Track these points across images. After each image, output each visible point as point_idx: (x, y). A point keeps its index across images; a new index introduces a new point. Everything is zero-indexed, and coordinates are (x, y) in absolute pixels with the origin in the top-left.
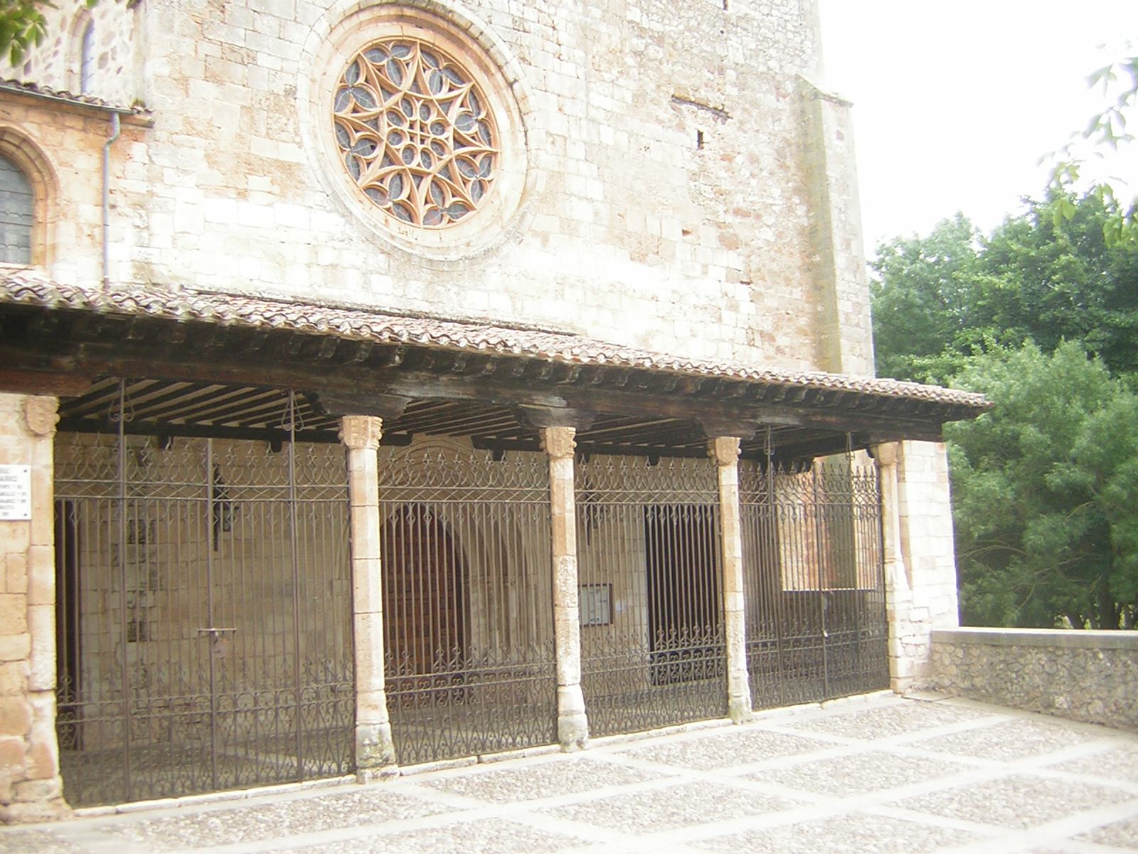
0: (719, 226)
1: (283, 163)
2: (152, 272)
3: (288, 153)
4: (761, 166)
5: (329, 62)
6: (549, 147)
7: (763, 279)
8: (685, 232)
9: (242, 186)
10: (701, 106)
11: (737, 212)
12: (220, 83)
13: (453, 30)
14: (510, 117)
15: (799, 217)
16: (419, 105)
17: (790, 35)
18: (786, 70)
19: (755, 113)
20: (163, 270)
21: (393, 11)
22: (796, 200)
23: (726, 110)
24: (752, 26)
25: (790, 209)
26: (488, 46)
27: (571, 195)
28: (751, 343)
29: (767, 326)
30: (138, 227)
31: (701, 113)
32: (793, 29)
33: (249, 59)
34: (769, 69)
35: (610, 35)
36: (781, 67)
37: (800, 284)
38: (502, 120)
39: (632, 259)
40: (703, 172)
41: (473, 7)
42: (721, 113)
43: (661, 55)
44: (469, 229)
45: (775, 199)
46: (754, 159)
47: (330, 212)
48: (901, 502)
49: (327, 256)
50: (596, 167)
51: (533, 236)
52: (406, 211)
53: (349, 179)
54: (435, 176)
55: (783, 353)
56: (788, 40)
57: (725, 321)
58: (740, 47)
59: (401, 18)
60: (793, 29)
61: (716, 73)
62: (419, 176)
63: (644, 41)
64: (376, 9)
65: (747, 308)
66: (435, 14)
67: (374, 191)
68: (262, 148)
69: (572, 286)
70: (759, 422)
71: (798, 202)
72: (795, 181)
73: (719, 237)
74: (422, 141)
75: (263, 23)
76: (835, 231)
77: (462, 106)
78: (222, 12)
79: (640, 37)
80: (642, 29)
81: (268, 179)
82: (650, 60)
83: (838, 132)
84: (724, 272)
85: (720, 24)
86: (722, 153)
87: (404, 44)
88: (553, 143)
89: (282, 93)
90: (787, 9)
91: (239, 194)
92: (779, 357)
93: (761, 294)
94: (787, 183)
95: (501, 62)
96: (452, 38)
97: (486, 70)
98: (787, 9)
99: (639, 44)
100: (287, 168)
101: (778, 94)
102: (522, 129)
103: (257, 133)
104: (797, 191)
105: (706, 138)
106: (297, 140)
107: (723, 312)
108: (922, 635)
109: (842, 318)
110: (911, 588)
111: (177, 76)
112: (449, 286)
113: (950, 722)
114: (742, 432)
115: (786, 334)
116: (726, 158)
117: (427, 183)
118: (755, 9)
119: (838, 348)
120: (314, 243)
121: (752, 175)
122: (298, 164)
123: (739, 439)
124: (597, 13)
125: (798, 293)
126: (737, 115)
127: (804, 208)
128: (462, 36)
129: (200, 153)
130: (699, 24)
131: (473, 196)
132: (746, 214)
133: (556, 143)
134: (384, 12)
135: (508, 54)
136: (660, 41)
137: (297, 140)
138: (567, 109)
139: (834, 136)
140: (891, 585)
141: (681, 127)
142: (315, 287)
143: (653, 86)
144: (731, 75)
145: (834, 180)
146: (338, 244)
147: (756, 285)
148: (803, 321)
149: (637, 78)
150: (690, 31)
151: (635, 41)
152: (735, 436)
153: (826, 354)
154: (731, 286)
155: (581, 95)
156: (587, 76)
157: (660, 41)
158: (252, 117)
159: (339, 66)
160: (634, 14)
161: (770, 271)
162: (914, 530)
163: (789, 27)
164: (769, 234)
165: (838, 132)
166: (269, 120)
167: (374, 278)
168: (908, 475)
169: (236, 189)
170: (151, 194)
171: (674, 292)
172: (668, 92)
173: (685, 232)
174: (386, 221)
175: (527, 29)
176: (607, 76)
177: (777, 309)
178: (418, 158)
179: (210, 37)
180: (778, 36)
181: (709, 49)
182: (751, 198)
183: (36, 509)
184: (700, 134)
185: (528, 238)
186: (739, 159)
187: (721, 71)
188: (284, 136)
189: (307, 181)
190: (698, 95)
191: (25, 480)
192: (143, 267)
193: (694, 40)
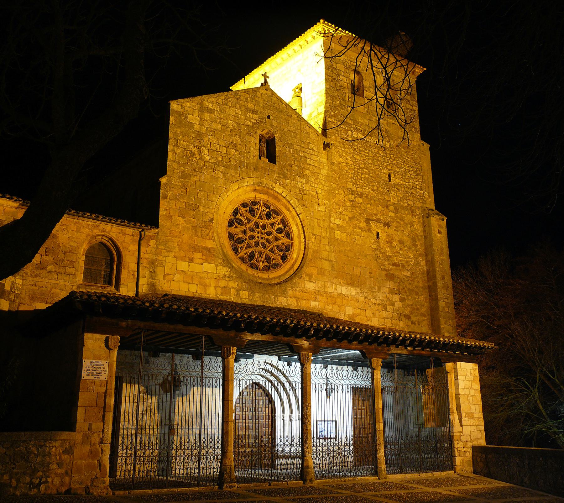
0: (386, 270)
1: (207, 248)
2: (155, 289)
3: (209, 244)
4: (405, 245)
5: (226, 209)
7: (406, 292)
9: (191, 257)
10: (378, 221)
12: (184, 218)
13: (276, 194)
14: (298, 228)
17: (418, 190)
19: (402, 223)
20: (160, 288)
22: (420, 259)
24: (401, 187)
25: (417, 263)
26: (289, 200)
27: (322, 259)
28: (399, 318)
29: (407, 312)
30: (151, 272)
31: (378, 224)
32: (420, 188)
34: (409, 205)
35: (340, 195)
36: (414, 203)
38: (294, 229)
39: (348, 284)
40: (379, 249)
41: (283, 185)
42: (387, 225)
43: (361, 201)
45: (411, 259)
46: (401, 242)
47: (224, 267)
48: (457, 388)
49: (223, 283)
51: (306, 275)
52: (255, 267)
53: (233, 253)
55: (415, 324)
56: (417, 192)
57: (388, 310)
58: (396, 196)
60: (420, 188)
63: (354, 196)
64: (245, 187)
65: (398, 304)
66: (268, 188)
70: (390, 352)
73: (386, 275)
75: (201, 194)
76: (437, 272)
77: (279, 224)
79: (353, 194)
80: (353, 191)
81: (201, 254)
83: (439, 230)
84: (388, 289)
86: (387, 240)
89: (207, 221)
91: (190, 259)
92: (413, 325)
93: (405, 299)
94: (417, 252)
96: (276, 198)
97: (289, 210)
100: (208, 250)
101: (413, 215)
102: (303, 233)
103: (197, 236)
104: (420, 255)
106: (213, 238)
107: (387, 306)
108: (467, 448)
109: (441, 309)
110: (462, 426)
112: (271, 295)
113: (473, 484)
114: (382, 357)
115: (416, 316)
116: (390, 242)
118: (403, 181)
119: (439, 321)
120: (218, 278)
121: (401, 249)
122: (213, 248)
123: (381, 359)
124: (335, 186)
125: (421, 298)
126: (395, 224)
127: (424, 262)
128: (279, 196)
129: (176, 245)
130: (378, 188)
131: (282, 259)
134: (248, 188)
136: (361, 195)
137: (213, 238)
138: (321, 224)
139: (437, 233)
140: (452, 424)
141: (369, 230)
142: (218, 296)
143: (357, 214)
144: (391, 208)
146: (227, 279)
147: (402, 295)
148: (423, 310)
149: (351, 211)
150: (374, 191)
151: (350, 196)
152: (380, 358)
153: (435, 326)
154: (391, 296)
155: (327, 219)
156: (330, 211)
157: (361, 195)
158: (196, 230)
159: (230, 210)
160: (350, 185)
161: (409, 289)
162: (462, 400)
163: (418, 187)
164: (408, 274)
165: (439, 230)
167: (241, 292)
168: (459, 377)
169: (189, 257)
170: (157, 260)
171: (366, 298)
172: (364, 217)
174: (247, 269)
177: (412, 305)
179: (181, 200)
180: (413, 191)
181: (382, 198)
182: (400, 258)
183: (110, 377)
184: (378, 234)
185: (304, 276)
186: (395, 243)
187: (387, 207)
189: (216, 254)
190: (377, 217)
191: (106, 366)
192: (152, 286)
193: (376, 195)
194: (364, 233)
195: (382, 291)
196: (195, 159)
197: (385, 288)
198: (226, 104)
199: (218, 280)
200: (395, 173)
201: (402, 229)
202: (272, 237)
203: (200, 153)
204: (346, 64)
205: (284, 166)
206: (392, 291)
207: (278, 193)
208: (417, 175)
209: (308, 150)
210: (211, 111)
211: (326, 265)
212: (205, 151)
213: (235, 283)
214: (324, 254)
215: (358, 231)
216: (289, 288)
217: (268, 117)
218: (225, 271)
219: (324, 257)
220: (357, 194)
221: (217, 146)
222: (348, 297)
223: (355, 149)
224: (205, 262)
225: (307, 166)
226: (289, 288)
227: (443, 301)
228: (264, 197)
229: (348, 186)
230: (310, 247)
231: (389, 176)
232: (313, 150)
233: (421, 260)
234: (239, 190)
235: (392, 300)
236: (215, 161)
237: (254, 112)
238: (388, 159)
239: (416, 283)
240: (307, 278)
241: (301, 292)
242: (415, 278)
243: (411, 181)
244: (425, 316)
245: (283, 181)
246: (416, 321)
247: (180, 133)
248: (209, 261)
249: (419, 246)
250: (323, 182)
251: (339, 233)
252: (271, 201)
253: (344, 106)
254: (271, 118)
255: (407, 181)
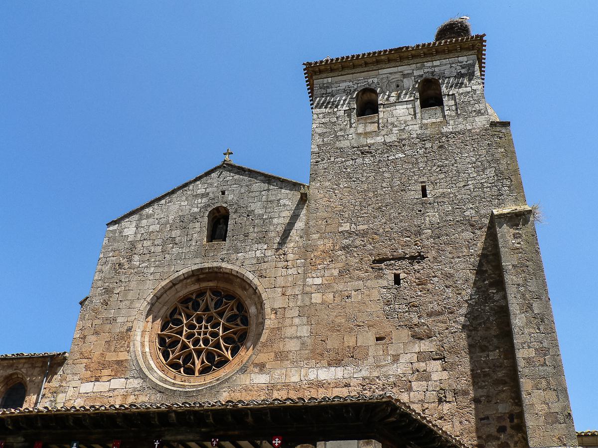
3: (123, 356)
6: (273, 316)
8: (378, 339)
11: (430, 315)
13: (226, 276)
15: (497, 301)
16: (205, 317)
18: (482, 212)
19: (449, 249)
21: (193, 279)
23: (422, 254)
27: (284, 339)
28: (440, 401)
33: (115, 320)
37: (498, 348)
38: (253, 310)
39: (329, 365)
42: (419, 258)
44: (222, 373)
50: (305, 319)
52: (190, 372)
54: (207, 349)
57: (414, 388)
59: (199, 280)
61: (412, 237)
62: (199, 352)
67: (175, 366)
68: (111, 357)
69: (279, 390)
71: (495, 291)
72: (492, 278)
74: (205, 333)
75: (122, 305)
78: (106, 306)
82: (356, 247)
85: (419, 207)
87: (201, 293)
88: (276, 313)
89: (125, 331)
90: (483, 176)
94: (484, 281)
95: (249, 282)
97: (244, 289)
98: (483, 176)
99: (346, 242)
100: (119, 363)
105: (402, 276)
109: (521, 363)
111: (82, 336)
117: (203, 355)
120: (125, 394)
128: (231, 277)
132: (439, 314)
133: (278, 313)
134: (188, 281)
135: (250, 276)
138: (289, 292)
145: (510, 267)
154: (424, 364)
157: (364, 234)
160: (346, 227)
166: (117, 344)
169: (95, 377)
171: (364, 379)
173: (378, 339)
174: (175, 377)
175: (266, 260)
176: (319, 267)
178: (201, 342)
180: (474, 194)
187: (419, 233)
188: (122, 349)
194: (369, 283)
195: (401, 360)
196: (123, 270)
197: (408, 354)
198: (170, 202)
199: (125, 397)
200: (436, 183)
201: (450, 256)
202: (219, 329)
203: (130, 260)
204: (350, 90)
205: (237, 239)
206: (422, 357)
207: (227, 273)
208: (483, 171)
209: (277, 208)
210: (148, 217)
211: (293, 346)
212: (136, 258)
213: (147, 395)
214: (290, 331)
215: (356, 283)
216: (224, 390)
217: (223, 193)
218: (136, 383)
219: (289, 335)
220: (357, 235)
221: (152, 248)
222: (329, 384)
223: (358, 179)
224: (113, 379)
225: (272, 228)
226: (224, 390)
227: (529, 347)
228: (211, 284)
229: (341, 229)
230: (266, 326)
231: (424, 190)
232: (284, 205)
233: (495, 291)
234: (176, 287)
235: (425, 371)
236: (146, 265)
237: (203, 196)
238: (422, 169)
239: (480, 333)
240: (257, 370)
241: (244, 393)
242: (480, 324)
243: (470, 182)
244: (504, 383)
245: (234, 256)
246: (481, 396)
247: (112, 250)
248: (119, 375)
249: (490, 272)
250: (297, 238)
251: (320, 295)
252: (222, 285)
253: (342, 136)
254: (226, 193)
255: (462, 184)
